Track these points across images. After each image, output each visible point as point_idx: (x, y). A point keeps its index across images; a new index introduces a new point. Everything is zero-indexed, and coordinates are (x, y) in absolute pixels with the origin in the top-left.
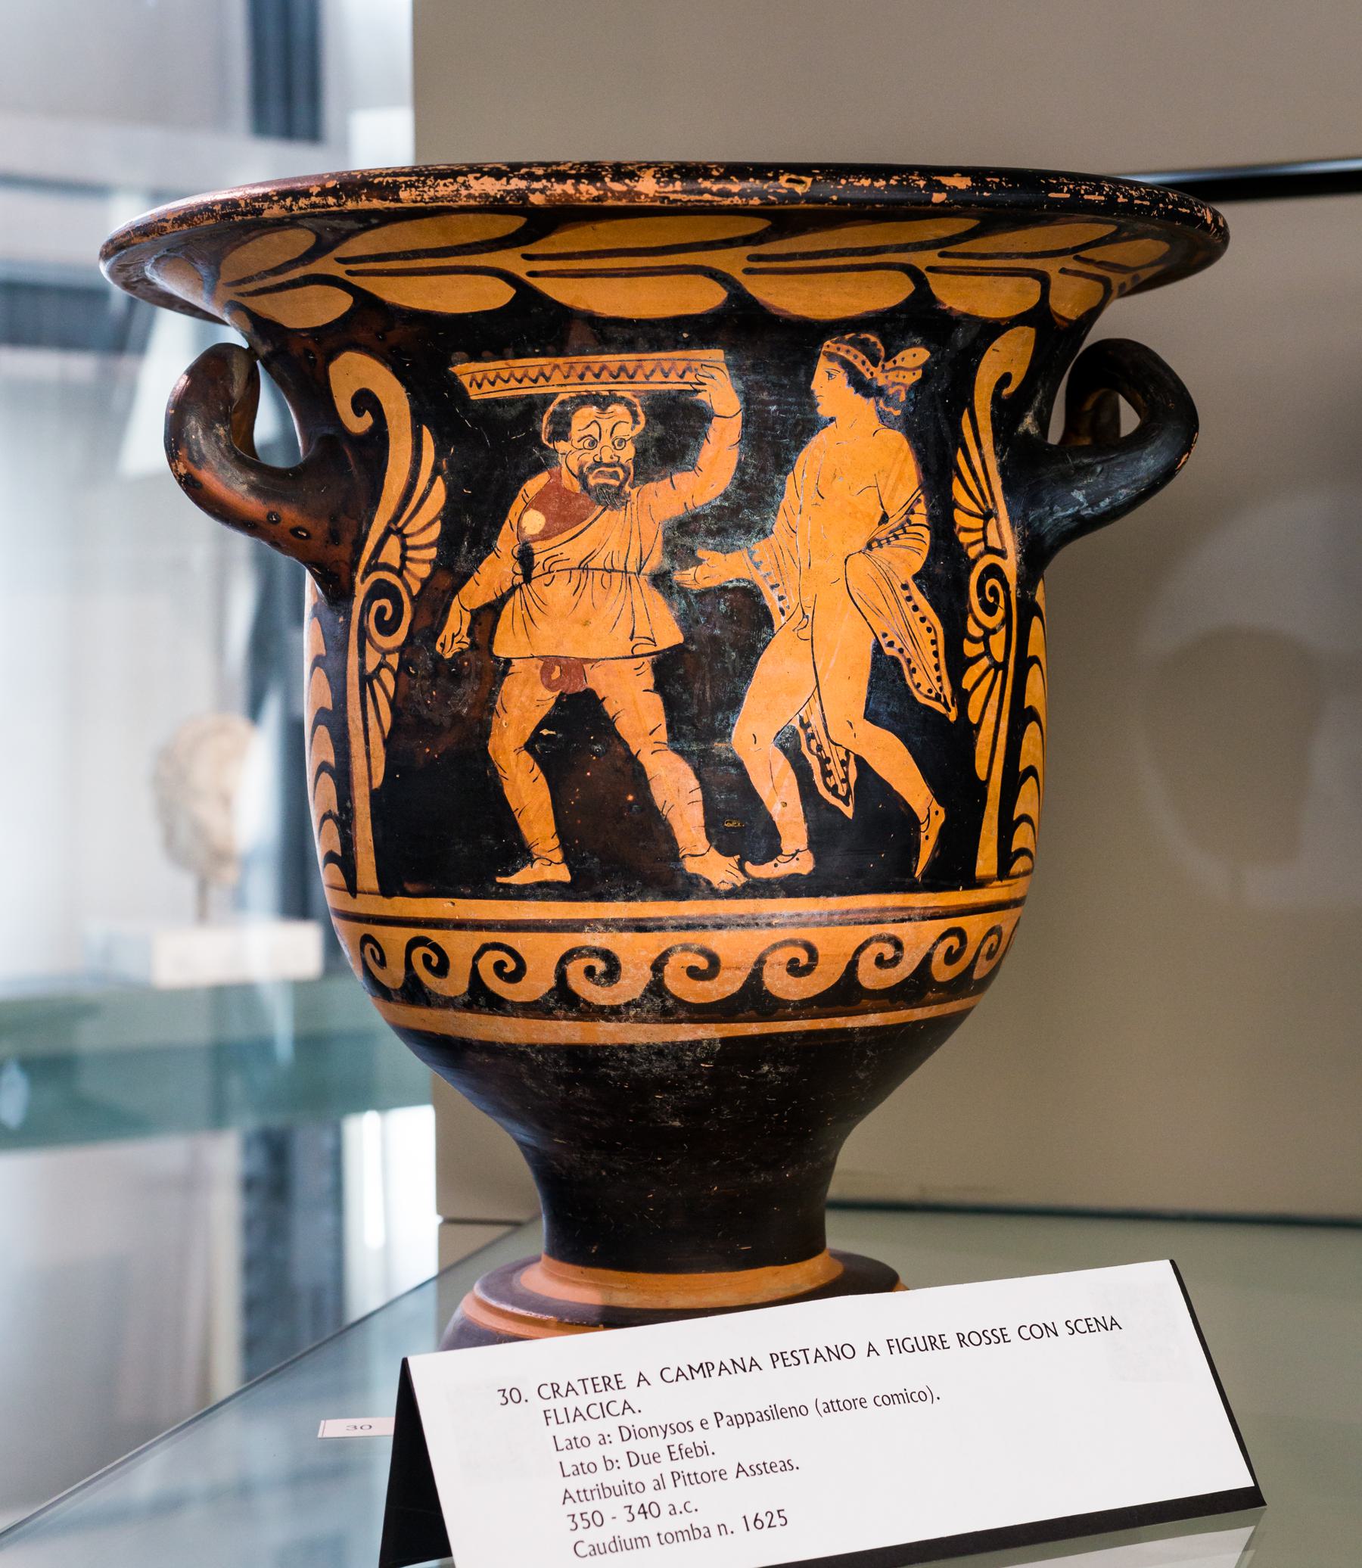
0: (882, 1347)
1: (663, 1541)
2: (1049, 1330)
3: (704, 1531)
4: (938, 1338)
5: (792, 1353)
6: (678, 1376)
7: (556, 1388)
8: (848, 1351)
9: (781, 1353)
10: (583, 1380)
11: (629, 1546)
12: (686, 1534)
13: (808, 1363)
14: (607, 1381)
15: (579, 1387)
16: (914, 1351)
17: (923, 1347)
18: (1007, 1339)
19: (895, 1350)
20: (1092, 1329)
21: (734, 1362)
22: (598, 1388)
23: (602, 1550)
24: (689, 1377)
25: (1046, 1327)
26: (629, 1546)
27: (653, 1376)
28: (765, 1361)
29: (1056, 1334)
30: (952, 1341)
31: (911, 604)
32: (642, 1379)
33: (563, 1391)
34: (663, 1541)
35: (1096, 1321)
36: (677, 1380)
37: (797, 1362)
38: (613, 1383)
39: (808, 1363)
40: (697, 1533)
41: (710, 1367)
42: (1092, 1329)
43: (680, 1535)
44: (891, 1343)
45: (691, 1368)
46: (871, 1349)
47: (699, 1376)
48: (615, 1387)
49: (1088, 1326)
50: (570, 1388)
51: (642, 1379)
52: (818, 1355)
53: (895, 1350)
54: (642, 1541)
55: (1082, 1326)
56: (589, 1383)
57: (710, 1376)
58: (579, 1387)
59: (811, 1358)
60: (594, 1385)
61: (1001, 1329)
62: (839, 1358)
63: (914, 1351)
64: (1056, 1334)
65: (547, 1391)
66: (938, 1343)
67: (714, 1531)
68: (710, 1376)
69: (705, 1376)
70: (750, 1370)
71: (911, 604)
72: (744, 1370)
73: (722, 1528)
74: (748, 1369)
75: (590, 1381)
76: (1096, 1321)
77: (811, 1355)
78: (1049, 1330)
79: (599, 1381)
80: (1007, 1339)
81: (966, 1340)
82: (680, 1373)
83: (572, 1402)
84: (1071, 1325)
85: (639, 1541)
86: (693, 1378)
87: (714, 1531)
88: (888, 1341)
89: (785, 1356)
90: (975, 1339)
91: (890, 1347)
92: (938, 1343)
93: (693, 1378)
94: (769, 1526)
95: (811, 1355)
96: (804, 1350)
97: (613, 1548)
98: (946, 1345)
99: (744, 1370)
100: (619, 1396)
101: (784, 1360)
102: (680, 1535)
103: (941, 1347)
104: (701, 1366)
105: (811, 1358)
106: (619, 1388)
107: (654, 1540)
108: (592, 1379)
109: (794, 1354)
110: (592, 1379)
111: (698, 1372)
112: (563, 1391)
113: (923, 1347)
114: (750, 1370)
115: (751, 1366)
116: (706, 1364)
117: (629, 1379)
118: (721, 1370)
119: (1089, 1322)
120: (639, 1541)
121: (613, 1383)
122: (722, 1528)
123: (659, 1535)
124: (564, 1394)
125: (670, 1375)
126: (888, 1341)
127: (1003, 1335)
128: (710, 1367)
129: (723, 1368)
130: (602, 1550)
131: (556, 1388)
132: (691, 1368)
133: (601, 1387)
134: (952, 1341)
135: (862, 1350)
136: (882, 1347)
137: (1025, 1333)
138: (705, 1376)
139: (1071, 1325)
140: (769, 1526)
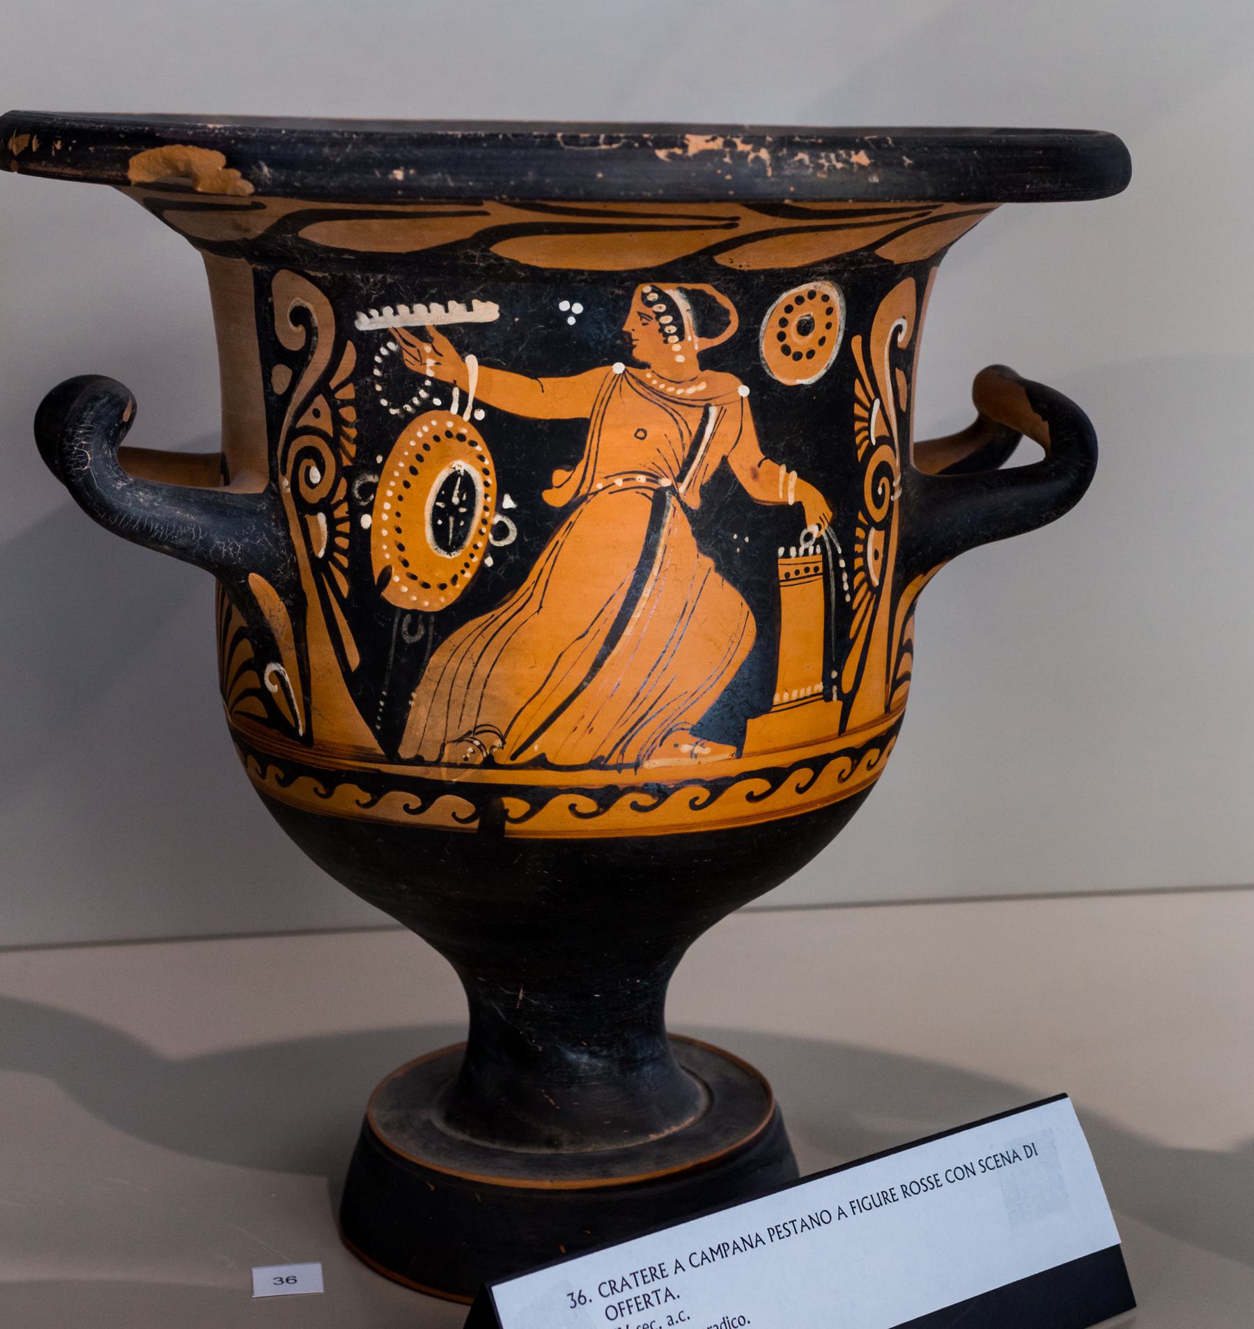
0: (848, 1210)
2: (968, 1170)
4: (889, 1192)
5: (784, 1226)
6: (703, 1259)
8: (826, 1217)
9: (776, 1227)
10: (634, 1274)
13: (796, 1233)
14: (653, 1270)
15: (631, 1281)
16: (871, 1208)
17: (878, 1203)
18: (939, 1183)
19: (857, 1210)
20: (999, 1164)
21: (743, 1240)
25: (966, 1168)
27: (685, 1264)
29: (974, 1173)
30: (899, 1193)
31: (787, 316)
32: (678, 1266)
35: (1002, 1156)
36: (702, 1264)
37: (788, 1234)
38: (658, 1273)
39: (796, 1233)
41: (726, 1248)
42: (999, 1164)
44: (854, 1205)
45: (711, 1250)
46: (841, 1213)
47: (718, 1257)
48: (660, 1276)
49: (996, 1161)
50: (625, 1283)
51: (678, 1266)
52: (804, 1225)
55: (991, 1163)
56: (639, 1276)
57: (726, 1256)
58: (631, 1281)
59: (799, 1228)
60: (643, 1277)
62: (819, 1224)
63: (871, 1208)
64: (974, 1173)
66: (890, 1197)
68: (726, 1256)
69: (723, 1257)
70: (756, 1246)
71: (787, 316)
74: (754, 1245)
75: (640, 1272)
76: (1002, 1156)
78: (968, 1170)
79: (647, 1273)
80: (939, 1183)
81: (909, 1191)
82: (704, 1257)
83: (627, 1294)
84: (983, 1163)
86: (714, 1260)
88: (850, 1203)
89: (779, 1229)
90: (915, 1188)
91: (853, 1208)
92: (890, 1197)
93: (714, 1260)
95: (798, 1224)
96: (792, 1222)
99: (752, 1246)
100: (659, 1284)
101: (778, 1233)
103: (892, 1200)
104: (719, 1247)
105: (799, 1229)
106: (663, 1277)
108: (641, 1271)
109: (786, 1226)
110: (641, 1271)
111: (717, 1254)
112: (618, 1287)
113: (878, 1203)
114: (756, 1246)
115: (757, 1241)
116: (723, 1244)
117: (669, 1268)
118: (734, 1249)
119: (997, 1158)
121: (658, 1273)
124: (620, 1290)
125: (696, 1260)
126: (850, 1203)
127: (936, 1181)
128: (726, 1248)
132: (711, 1250)
133: (649, 1278)
134: (899, 1193)
135: (835, 1214)
136: (848, 1210)
137: (951, 1176)
138: (723, 1257)
139: (983, 1163)
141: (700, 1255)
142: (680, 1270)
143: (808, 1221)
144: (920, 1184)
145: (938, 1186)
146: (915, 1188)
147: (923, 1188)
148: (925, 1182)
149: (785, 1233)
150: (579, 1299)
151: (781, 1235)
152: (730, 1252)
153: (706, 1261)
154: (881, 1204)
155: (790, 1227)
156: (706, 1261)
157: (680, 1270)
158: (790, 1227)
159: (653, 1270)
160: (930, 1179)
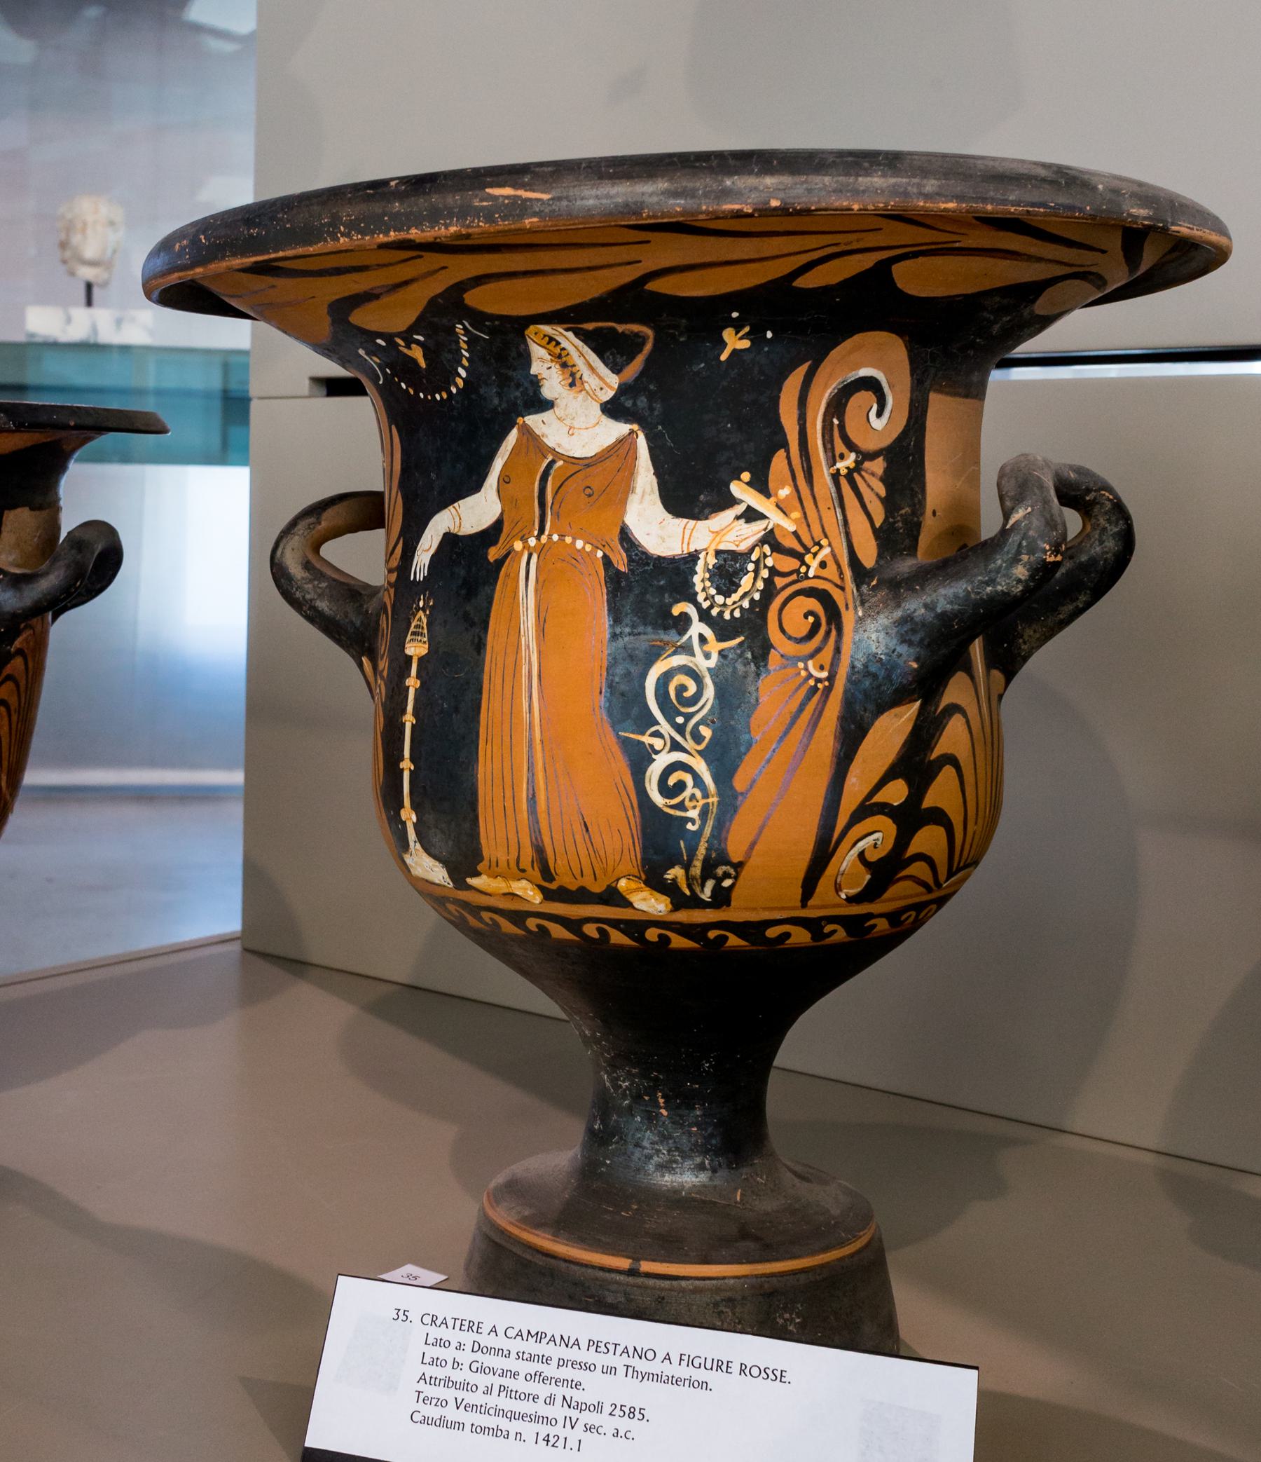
1: (474, 1430)
3: (506, 1433)
7: (434, 1319)
8: (650, 1355)
11: (449, 1426)
12: (491, 1431)
14: (471, 1324)
15: (451, 1323)
17: (709, 1366)
19: (684, 1363)
22: (463, 1328)
23: (430, 1422)
24: (525, 1338)
26: (449, 1426)
27: (501, 1331)
28: (584, 1345)
30: (735, 1368)
32: (494, 1330)
33: (438, 1323)
34: (474, 1430)
38: (475, 1328)
40: (499, 1433)
41: (544, 1335)
43: (487, 1430)
45: (529, 1332)
47: (531, 1340)
48: (475, 1331)
50: (445, 1322)
53: (684, 1363)
54: (460, 1425)
56: (458, 1323)
58: (451, 1323)
61: (782, 1371)
62: (640, 1358)
65: (427, 1320)
67: (512, 1435)
72: (567, 1346)
73: (519, 1435)
74: (570, 1346)
77: (619, 1350)
79: (466, 1323)
81: (747, 1371)
82: (520, 1334)
83: (441, 1333)
85: (457, 1425)
87: (512, 1435)
90: (755, 1372)
91: (681, 1359)
94: (553, 1446)
95: (619, 1350)
96: (616, 1345)
97: (438, 1424)
98: (729, 1370)
99: (567, 1346)
102: (487, 1430)
104: (537, 1334)
107: (468, 1427)
109: (607, 1345)
112: (438, 1323)
113: (709, 1366)
117: (486, 1328)
120: (457, 1425)
121: (475, 1328)
122: (519, 1435)
123: (472, 1425)
125: (511, 1333)
128: (544, 1335)
129: (553, 1339)
130: (430, 1422)
131: (434, 1319)
132: (529, 1332)
133: (466, 1328)
134: (735, 1368)
135: (660, 1356)
140: (553, 1446)
141: (516, 1331)
142: (493, 1334)
143: (631, 1351)
144: (762, 1371)
145: (781, 1381)
146: (755, 1372)
147: (763, 1374)
148: (769, 1372)
149: (603, 1349)
150: (402, 1315)
151: (599, 1350)
152: (544, 1341)
153: (519, 1338)
154: (712, 1369)
155: (611, 1348)
156: (519, 1338)
157: (493, 1334)
158: (611, 1348)
159: (471, 1324)
160: (775, 1372)
